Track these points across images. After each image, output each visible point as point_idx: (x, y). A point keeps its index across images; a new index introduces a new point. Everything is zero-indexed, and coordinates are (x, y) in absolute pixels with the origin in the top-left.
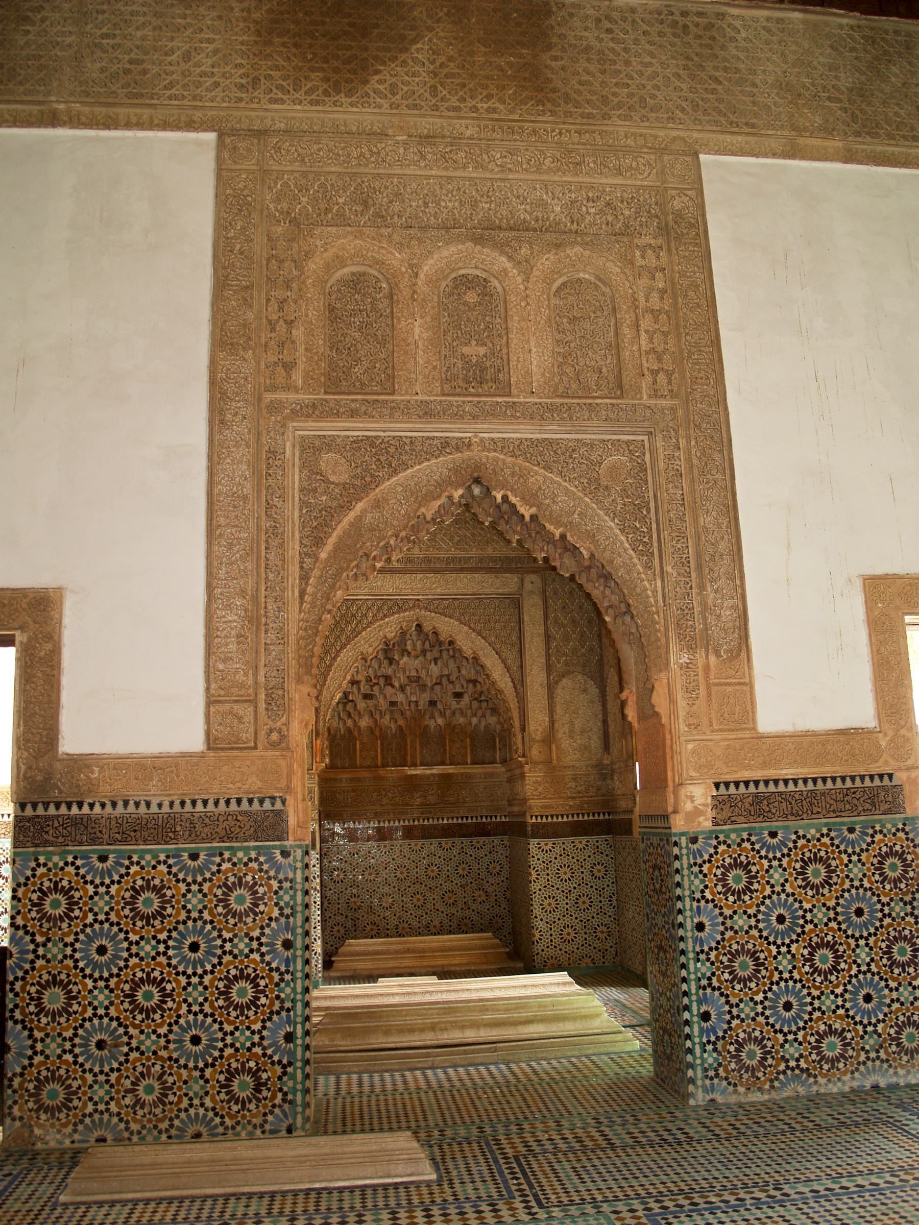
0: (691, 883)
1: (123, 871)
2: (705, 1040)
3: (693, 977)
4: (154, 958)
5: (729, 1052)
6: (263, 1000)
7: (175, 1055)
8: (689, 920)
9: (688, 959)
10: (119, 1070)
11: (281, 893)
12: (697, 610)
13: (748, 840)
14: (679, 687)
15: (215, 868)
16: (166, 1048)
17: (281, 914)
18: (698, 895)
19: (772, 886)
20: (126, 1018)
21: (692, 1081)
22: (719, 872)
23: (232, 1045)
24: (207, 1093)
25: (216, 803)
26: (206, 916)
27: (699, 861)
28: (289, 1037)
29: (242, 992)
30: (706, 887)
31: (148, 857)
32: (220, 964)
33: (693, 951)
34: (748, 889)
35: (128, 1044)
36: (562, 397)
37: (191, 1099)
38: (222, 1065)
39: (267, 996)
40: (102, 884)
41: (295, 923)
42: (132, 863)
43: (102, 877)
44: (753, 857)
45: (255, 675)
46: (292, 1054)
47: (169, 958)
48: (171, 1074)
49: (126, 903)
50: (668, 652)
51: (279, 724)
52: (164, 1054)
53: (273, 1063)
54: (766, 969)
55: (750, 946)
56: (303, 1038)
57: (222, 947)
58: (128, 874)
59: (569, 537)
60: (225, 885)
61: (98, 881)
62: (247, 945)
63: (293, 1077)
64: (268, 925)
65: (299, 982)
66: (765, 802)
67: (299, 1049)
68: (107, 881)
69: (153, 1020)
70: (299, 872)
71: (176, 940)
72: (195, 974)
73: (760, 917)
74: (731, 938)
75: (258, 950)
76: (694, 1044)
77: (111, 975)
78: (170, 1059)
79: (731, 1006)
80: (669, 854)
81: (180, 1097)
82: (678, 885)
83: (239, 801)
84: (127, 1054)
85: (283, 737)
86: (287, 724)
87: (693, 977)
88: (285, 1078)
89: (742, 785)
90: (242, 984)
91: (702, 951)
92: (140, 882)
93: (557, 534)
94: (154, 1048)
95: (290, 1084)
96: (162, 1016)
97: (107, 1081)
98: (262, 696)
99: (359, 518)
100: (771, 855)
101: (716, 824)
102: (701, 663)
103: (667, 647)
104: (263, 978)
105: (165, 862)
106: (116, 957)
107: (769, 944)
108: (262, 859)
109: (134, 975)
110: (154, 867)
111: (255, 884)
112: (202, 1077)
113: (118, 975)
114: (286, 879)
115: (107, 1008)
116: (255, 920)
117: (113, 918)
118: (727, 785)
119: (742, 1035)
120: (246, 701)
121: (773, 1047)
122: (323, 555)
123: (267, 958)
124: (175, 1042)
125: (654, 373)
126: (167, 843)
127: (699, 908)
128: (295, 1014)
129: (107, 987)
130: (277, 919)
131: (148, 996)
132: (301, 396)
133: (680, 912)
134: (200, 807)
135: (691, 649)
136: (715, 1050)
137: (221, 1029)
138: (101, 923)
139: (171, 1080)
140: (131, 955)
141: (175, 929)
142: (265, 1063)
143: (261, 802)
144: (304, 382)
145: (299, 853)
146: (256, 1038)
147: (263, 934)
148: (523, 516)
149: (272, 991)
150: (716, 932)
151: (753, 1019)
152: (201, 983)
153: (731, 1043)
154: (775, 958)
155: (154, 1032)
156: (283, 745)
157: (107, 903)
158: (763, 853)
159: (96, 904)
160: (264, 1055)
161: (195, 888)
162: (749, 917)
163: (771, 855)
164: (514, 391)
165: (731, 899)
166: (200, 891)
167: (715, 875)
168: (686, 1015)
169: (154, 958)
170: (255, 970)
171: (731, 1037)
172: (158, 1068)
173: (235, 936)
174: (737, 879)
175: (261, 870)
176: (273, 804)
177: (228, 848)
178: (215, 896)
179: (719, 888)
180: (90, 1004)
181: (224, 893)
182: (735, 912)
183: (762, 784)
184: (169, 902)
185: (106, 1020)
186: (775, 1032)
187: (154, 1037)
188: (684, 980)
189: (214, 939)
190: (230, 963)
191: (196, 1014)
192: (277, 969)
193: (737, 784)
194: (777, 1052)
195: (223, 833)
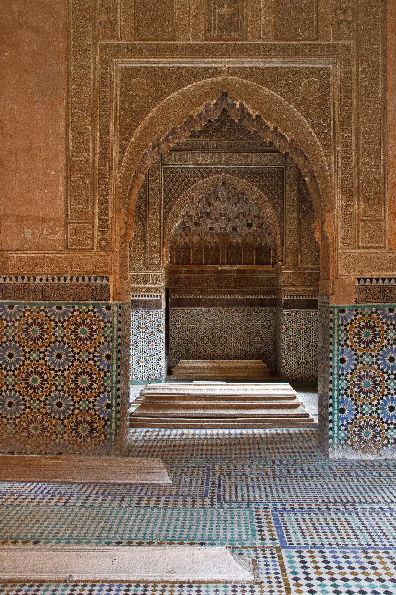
0: (339, 335)
1: (22, 314)
2: (340, 424)
3: (336, 388)
4: (38, 361)
5: (354, 431)
6: (95, 386)
7: (49, 412)
8: (336, 356)
9: (334, 378)
10: (20, 418)
11: (106, 329)
12: (355, 174)
13: (376, 313)
14: (339, 220)
15: (70, 314)
16: (44, 408)
17: (106, 341)
18: (342, 343)
19: (388, 340)
20: (24, 391)
21: (332, 446)
22: (356, 330)
23: (78, 408)
24: (65, 432)
25: (71, 279)
26: (65, 339)
27: (345, 323)
28: (109, 406)
29: (84, 381)
30: (348, 338)
31: (35, 307)
32: (73, 365)
33: (337, 374)
34: (373, 341)
35: (25, 405)
36: (279, 40)
37: (57, 435)
38: (73, 418)
39: (97, 384)
40: (11, 321)
41: (113, 345)
42: (26, 310)
43: (11, 317)
44: (378, 323)
45: (93, 208)
46: (110, 415)
47: (46, 361)
48: (46, 421)
49: (24, 332)
50: (334, 200)
51: (106, 236)
52: (43, 410)
53: (100, 419)
54: (381, 387)
55: (372, 373)
56: (116, 407)
57: (74, 356)
58: (24, 316)
59: (279, 130)
60: (76, 324)
61: (8, 319)
62: (87, 356)
63: (110, 426)
64: (98, 346)
65: (114, 377)
66: (388, 291)
67: (114, 413)
68: (13, 319)
69: (38, 393)
70: (115, 318)
71: (49, 352)
72: (59, 370)
73: (379, 357)
74: (360, 368)
75: (93, 359)
76: (334, 425)
77: (16, 369)
78: (46, 413)
79: (358, 406)
80: (328, 318)
81: (51, 433)
82: (331, 336)
83: (83, 279)
84: (24, 410)
85: (108, 243)
86: (110, 236)
87: (336, 388)
88: (106, 427)
89: (374, 281)
90: (84, 376)
91: (343, 374)
92: (30, 321)
93: (272, 126)
94: (38, 407)
95: (109, 430)
96: (42, 391)
97: (14, 423)
98: (97, 220)
99: (154, 118)
100: (389, 322)
101: (356, 302)
102: (355, 207)
103: (335, 197)
104: (95, 374)
105: (44, 310)
106: (18, 359)
107: (383, 373)
108: (95, 310)
109: (28, 369)
110: (38, 313)
111: (92, 324)
112: (63, 424)
113: (19, 369)
114: (109, 322)
115: (13, 386)
116: (91, 343)
117: (17, 339)
118: (365, 280)
119: (363, 423)
120: (87, 223)
121: (381, 431)
122: (133, 139)
123: (98, 364)
124: (49, 405)
125: (339, 23)
126: (45, 300)
127: (342, 350)
128: (112, 394)
129: (14, 375)
130: (103, 343)
131: (35, 380)
132: (120, 42)
133: (331, 351)
134: (62, 281)
135: (349, 197)
136: (346, 429)
137: (73, 400)
138: (11, 341)
139: (47, 424)
140: (26, 359)
141: (49, 346)
142: (96, 419)
143: (96, 279)
144: (122, 33)
145: (116, 308)
146: (91, 406)
147: (95, 351)
148: (251, 116)
149: (100, 381)
150: (352, 364)
151: (370, 415)
152: (62, 375)
153: (356, 427)
154: (386, 381)
155: (38, 399)
156: (108, 248)
157: (13, 331)
158: (384, 321)
159: (8, 331)
160: (95, 414)
161: (59, 324)
162: (373, 357)
163: (389, 322)
164: (249, 37)
165: (362, 346)
166: (62, 326)
167: (354, 332)
168: (331, 409)
169: (38, 361)
170: (91, 370)
171: (356, 423)
172: (40, 417)
173: (81, 351)
174: (367, 335)
175: (95, 316)
176: (102, 281)
177: (77, 304)
178: (70, 329)
179: (356, 339)
180: (5, 383)
181: (75, 328)
182: (364, 354)
183: (387, 281)
184: (46, 331)
185: (13, 392)
186: (383, 422)
187: (38, 402)
188: (331, 390)
189: (69, 352)
190: (77, 365)
191: (59, 391)
192: (103, 370)
193: (371, 280)
194: (383, 434)
195: (74, 296)
